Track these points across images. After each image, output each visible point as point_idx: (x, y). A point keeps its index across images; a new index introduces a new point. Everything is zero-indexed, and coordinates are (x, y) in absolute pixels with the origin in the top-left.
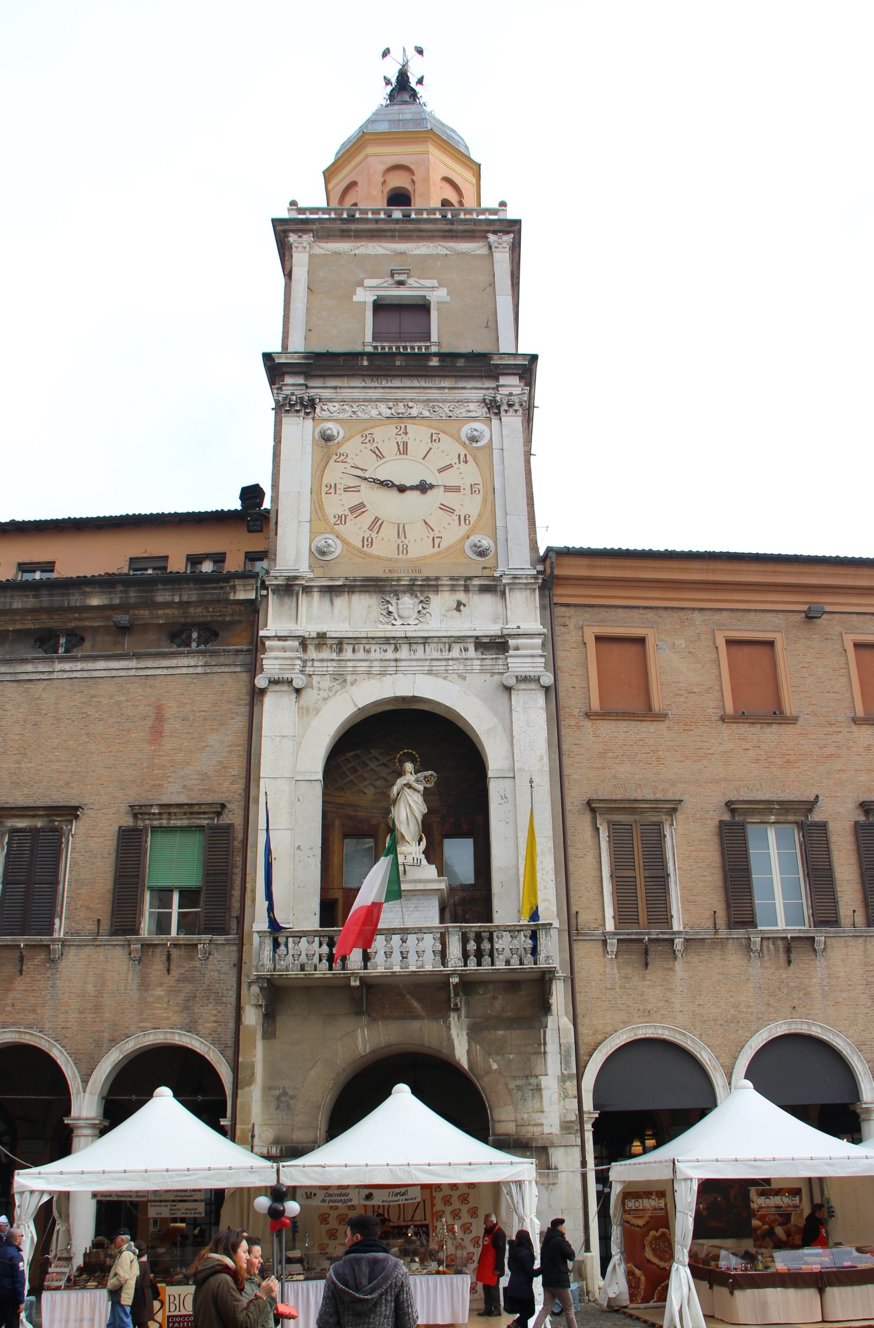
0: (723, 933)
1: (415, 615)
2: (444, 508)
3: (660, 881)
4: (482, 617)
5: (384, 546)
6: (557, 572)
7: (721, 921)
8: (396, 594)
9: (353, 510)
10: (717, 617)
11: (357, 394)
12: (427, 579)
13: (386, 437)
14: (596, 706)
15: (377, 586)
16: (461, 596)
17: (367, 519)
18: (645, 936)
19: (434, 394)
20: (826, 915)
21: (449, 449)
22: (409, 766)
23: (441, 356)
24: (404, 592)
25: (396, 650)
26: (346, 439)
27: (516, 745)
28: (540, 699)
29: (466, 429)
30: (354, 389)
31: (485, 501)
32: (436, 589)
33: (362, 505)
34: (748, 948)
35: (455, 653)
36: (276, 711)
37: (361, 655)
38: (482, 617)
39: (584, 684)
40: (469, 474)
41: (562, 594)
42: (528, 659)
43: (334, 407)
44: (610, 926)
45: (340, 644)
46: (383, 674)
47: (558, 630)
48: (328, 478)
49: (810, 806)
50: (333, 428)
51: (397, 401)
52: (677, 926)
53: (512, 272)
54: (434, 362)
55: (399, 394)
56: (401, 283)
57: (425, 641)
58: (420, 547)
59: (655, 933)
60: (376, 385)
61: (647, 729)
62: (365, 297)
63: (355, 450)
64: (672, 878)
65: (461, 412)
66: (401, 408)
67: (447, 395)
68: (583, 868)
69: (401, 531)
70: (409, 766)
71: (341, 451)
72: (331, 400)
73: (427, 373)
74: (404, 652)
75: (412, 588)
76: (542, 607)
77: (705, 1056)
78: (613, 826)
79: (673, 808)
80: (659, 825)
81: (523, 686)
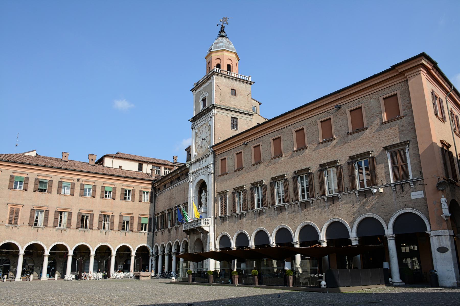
10: (235, 149)
19: (206, 118)
30: (198, 121)
41: (217, 153)
43: (197, 126)
44: (220, 215)
47: (216, 160)
50: (196, 131)
53: (225, 77)
57: (202, 169)
61: (227, 176)
62: (201, 100)
73: (205, 114)
78: (221, 196)
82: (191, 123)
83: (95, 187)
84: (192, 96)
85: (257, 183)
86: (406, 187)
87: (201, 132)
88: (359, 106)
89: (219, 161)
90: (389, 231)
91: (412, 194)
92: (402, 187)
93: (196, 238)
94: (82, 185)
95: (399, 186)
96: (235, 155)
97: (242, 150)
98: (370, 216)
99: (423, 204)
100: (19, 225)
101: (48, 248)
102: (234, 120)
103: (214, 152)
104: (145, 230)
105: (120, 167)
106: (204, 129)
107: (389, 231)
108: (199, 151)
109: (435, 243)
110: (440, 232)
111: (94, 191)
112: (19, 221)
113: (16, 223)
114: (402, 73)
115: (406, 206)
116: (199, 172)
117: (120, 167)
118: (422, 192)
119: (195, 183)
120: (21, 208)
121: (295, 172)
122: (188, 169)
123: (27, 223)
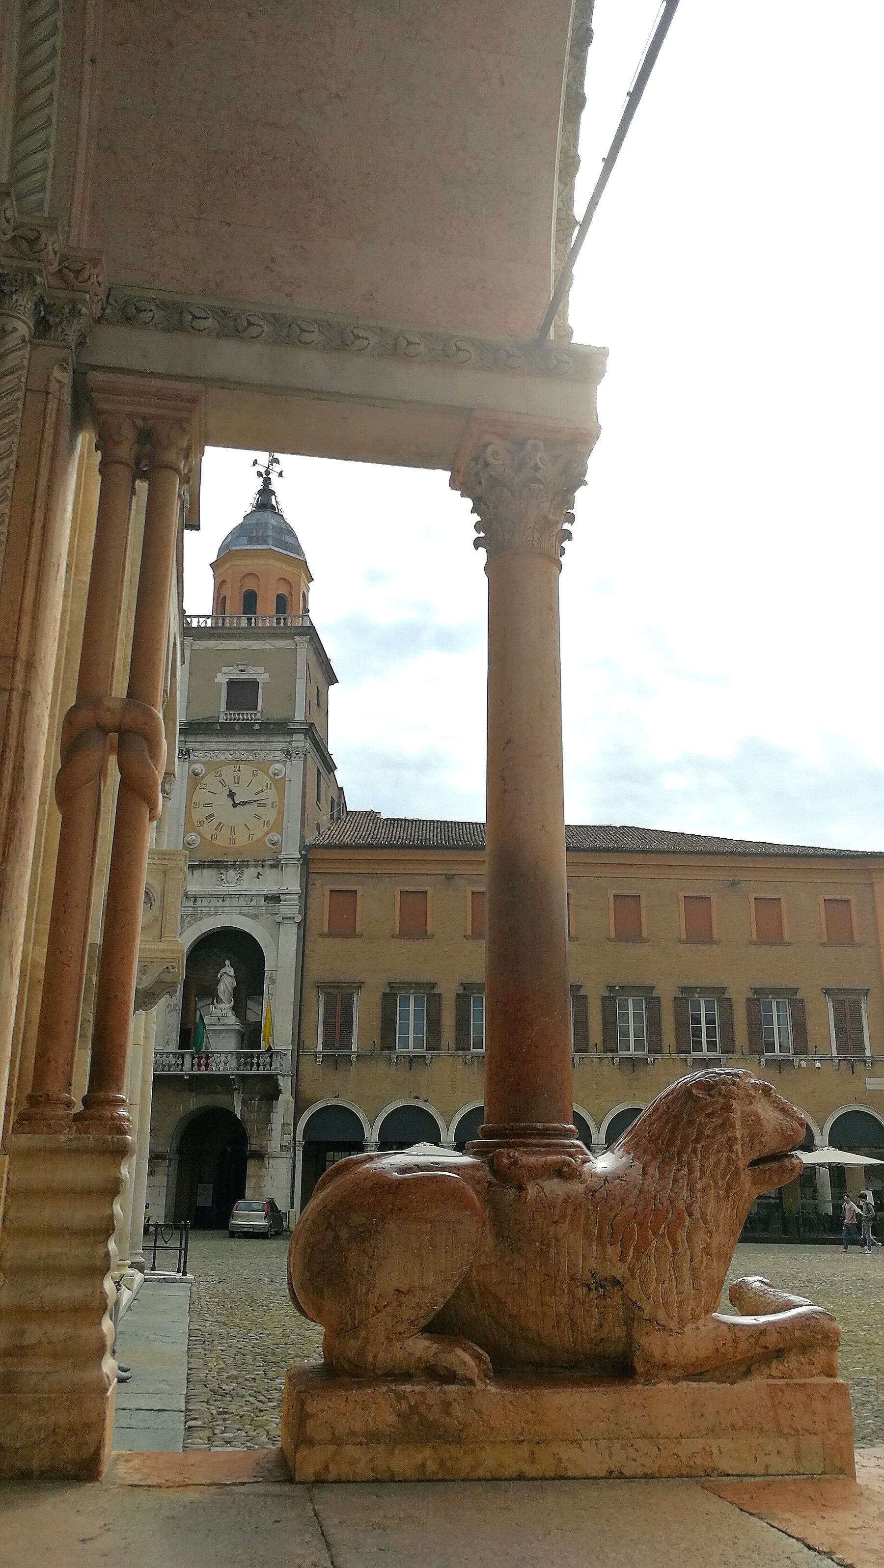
0: (377, 1052)
1: (235, 880)
2: (257, 817)
3: (348, 1023)
4: (270, 882)
5: (223, 841)
6: (309, 857)
7: (378, 1047)
8: (226, 868)
9: (207, 818)
11: (213, 746)
12: (243, 861)
13: (228, 773)
14: (326, 929)
15: (216, 865)
16: (260, 870)
17: (215, 823)
18: (337, 1054)
19: (256, 746)
20: (434, 1045)
21: (263, 780)
22: (227, 962)
24: (231, 868)
25: (224, 900)
26: (206, 774)
27: (280, 954)
28: (295, 929)
29: (272, 770)
30: (213, 743)
31: (278, 811)
32: (247, 866)
33: (212, 815)
35: (253, 903)
37: (205, 903)
38: (270, 882)
39: (321, 919)
40: (271, 795)
42: (291, 908)
44: (320, 1048)
45: (195, 898)
46: (216, 914)
47: (310, 887)
48: (194, 799)
49: (433, 985)
50: (198, 767)
51: (236, 750)
52: (354, 1048)
54: (257, 727)
55: (238, 746)
56: (243, 671)
57: (239, 896)
58: (242, 840)
60: (224, 739)
62: (222, 679)
63: (211, 781)
64: (354, 1023)
65: (271, 757)
66: (237, 754)
67: (263, 746)
68: (308, 1018)
69: (233, 831)
70: (227, 962)
71: (203, 781)
72: (199, 750)
73: (254, 733)
74: (227, 903)
75: (234, 866)
77: (361, 1116)
78: (328, 995)
79: (360, 986)
80: (351, 996)
81: (286, 921)
89: (322, 891)
93: (193, 1103)
95: (845, 1063)
96: (398, 894)
121: (611, 988)
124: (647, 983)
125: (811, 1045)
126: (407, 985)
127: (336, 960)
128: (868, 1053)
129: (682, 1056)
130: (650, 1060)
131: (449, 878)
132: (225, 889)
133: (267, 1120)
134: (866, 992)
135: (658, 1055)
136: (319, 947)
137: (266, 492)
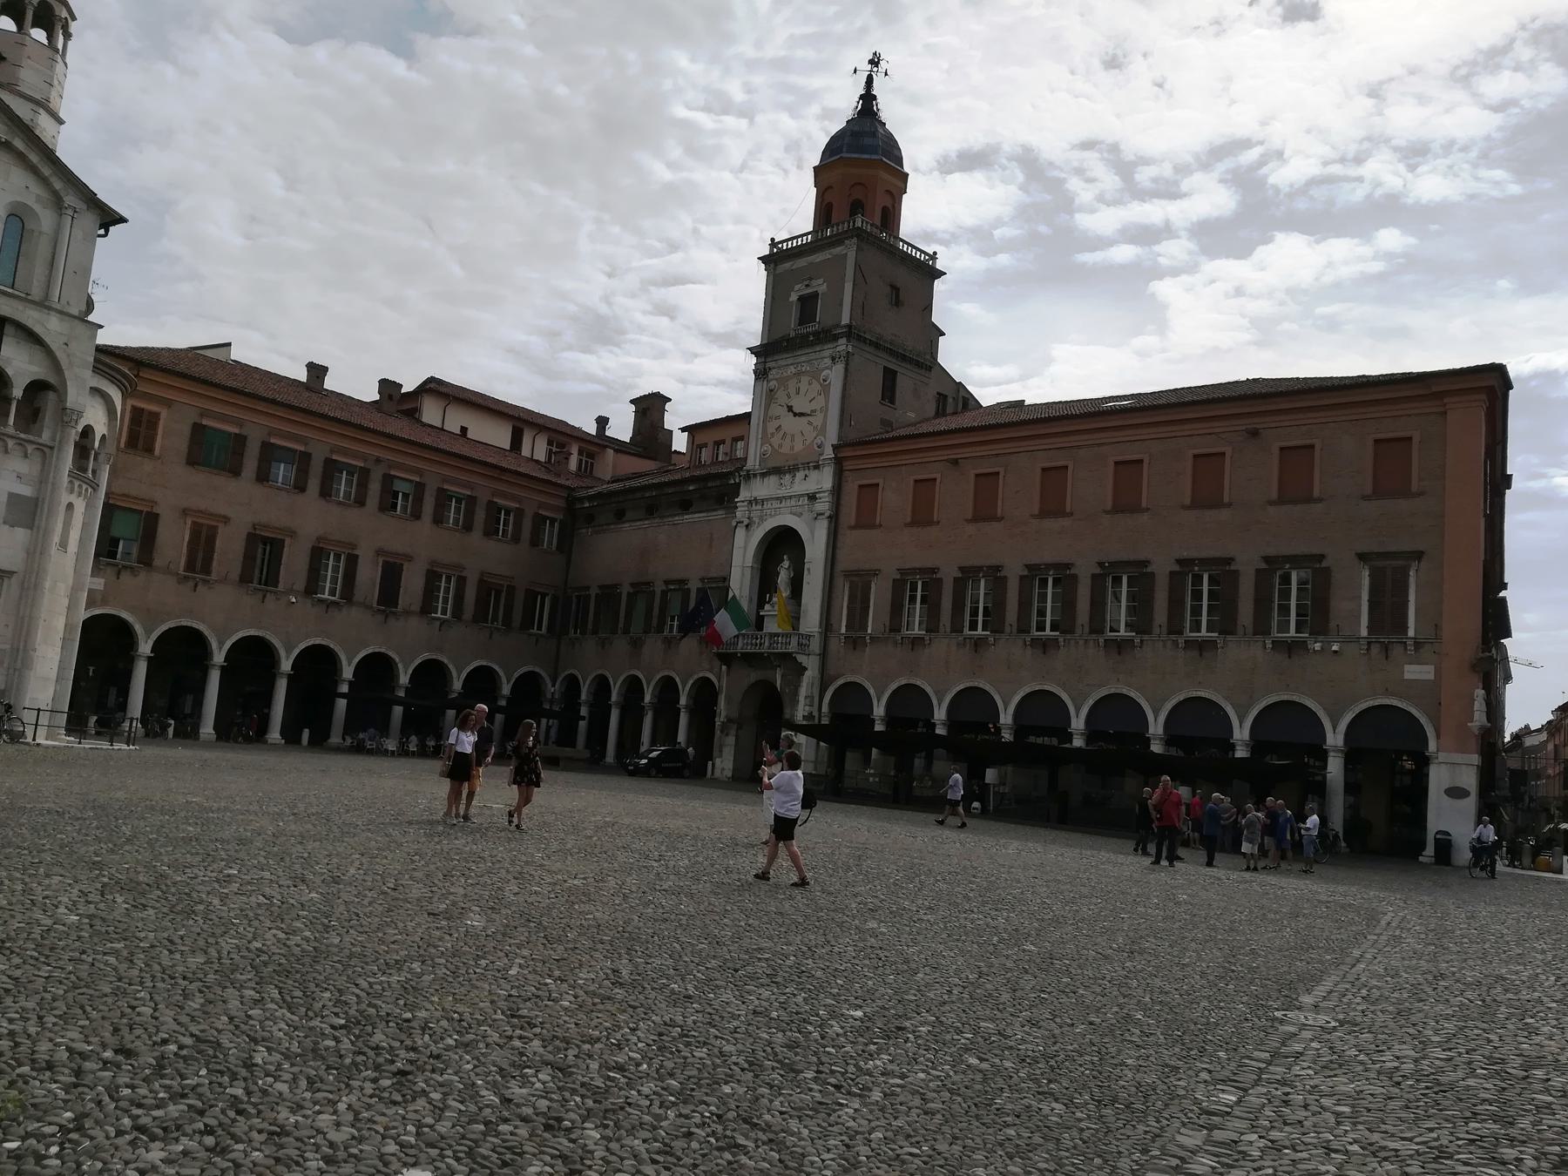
15: (778, 471)
19: (813, 356)
23: (815, 334)
34: (896, 643)
36: (740, 533)
39: (849, 514)
40: (821, 401)
41: (848, 465)
42: (824, 505)
44: (843, 630)
50: (773, 384)
58: (799, 447)
59: (859, 634)
62: (794, 297)
63: (781, 396)
73: (812, 344)
76: (835, 474)
77: (872, 691)
78: (851, 583)
79: (875, 573)
82: (754, 360)
83: (420, 487)
84: (760, 275)
85: (980, 568)
86: (1397, 651)
87: (792, 391)
88: (1308, 442)
90: (1335, 738)
91: (1407, 667)
92: (1386, 649)
93: (753, 676)
94: (388, 480)
97: (938, 476)
98: (1295, 698)
99: (1430, 694)
100: (214, 576)
101: (289, 652)
102: (890, 377)
103: (839, 462)
104: (540, 628)
105: (464, 430)
106: (804, 386)
107: (1335, 738)
108: (780, 446)
109: (1438, 778)
110: (1457, 757)
111: (419, 500)
112: (215, 564)
113: (207, 569)
114: (1439, 396)
115: (1387, 692)
116: (776, 504)
117: (464, 430)
118: (1431, 668)
119: (758, 534)
120: (221, 526)
121: (1101, 564)
122: (738, 485)
123: (235, 573)
124: (1142, 558)
125: (1333, 624)
126: (914, 571)
127: (858, 550)
128: (1411, 633)
129: (1173, 637)
130: (1137, 641)
131: (955, 462)
132: (782, 492)
133: (796, 693)
134: (1418, 555)
135: (1146, 637)
136: (848, 538)
137: (868, 98)
